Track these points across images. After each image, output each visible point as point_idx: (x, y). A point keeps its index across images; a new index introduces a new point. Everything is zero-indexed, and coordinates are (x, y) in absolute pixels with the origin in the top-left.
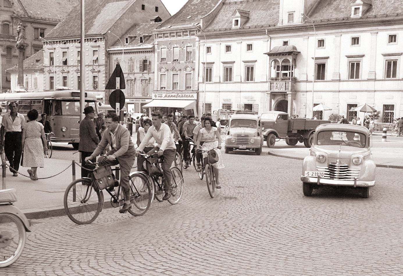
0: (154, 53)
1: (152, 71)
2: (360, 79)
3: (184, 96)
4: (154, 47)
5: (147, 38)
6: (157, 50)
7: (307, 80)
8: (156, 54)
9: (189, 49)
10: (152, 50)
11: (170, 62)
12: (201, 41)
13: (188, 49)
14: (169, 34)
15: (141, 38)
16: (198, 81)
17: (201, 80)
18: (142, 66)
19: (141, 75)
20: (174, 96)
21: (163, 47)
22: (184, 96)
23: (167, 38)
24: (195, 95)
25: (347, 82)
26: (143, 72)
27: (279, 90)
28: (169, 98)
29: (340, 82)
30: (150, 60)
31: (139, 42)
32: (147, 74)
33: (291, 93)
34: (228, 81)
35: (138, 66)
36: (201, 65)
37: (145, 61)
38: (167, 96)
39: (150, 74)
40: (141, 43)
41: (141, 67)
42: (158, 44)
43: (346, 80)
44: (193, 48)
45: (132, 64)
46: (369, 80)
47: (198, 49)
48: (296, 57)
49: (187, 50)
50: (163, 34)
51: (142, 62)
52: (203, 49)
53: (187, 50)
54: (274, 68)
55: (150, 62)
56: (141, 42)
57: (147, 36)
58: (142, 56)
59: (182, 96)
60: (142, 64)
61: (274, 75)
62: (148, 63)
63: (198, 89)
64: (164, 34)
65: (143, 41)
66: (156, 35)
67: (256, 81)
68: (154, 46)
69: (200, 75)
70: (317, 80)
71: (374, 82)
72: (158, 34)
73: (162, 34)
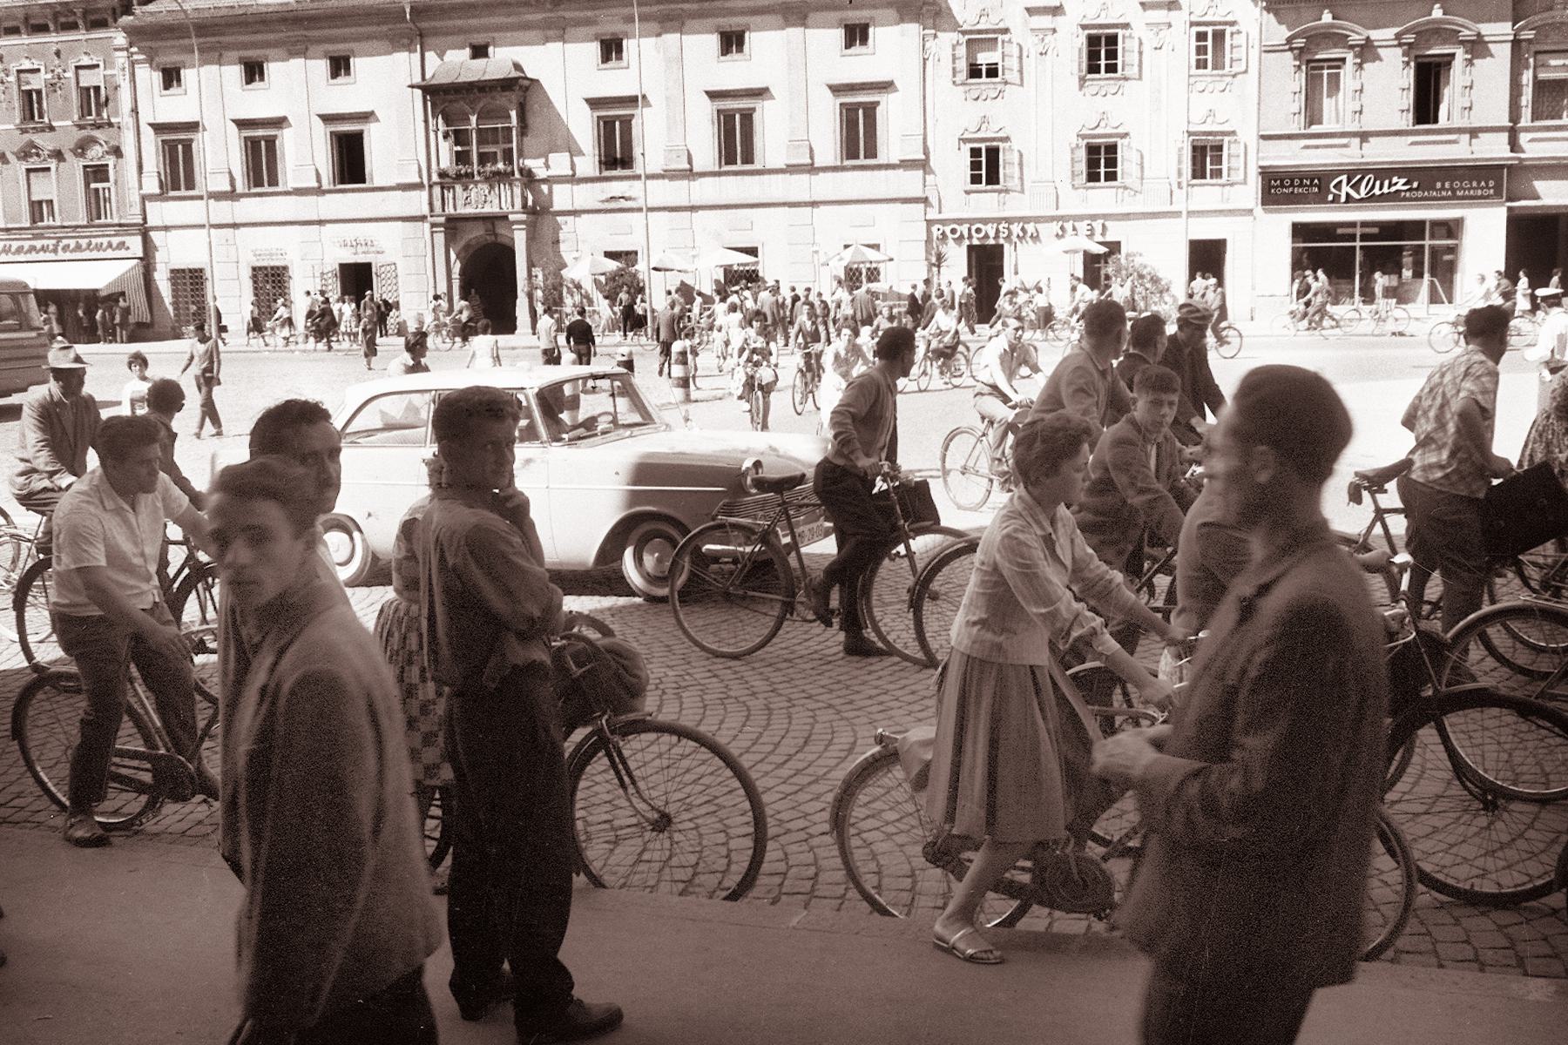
2: (757, 166)
3: (84, 246)
9: (88, 79)
13: (81, 79)
16: (141, 187)
17: (152, 186)
20: (44, 249)
22: (84, 246)
24: (135, 244)
25: (717, 178)
27: (478, 211)
28: (22, 257)
33: (524, 217)
36: (148, 135)
38: (13, 249)
44: (109, 72)
47: (127, 77)
49: (78, 83)
53: (78, 83)
54: (446, 136)
59: (78, 248)
61: (446, 161)
63: (145, 219)
67: (377, 183)
69: (145, 169)
70: (607, 173)
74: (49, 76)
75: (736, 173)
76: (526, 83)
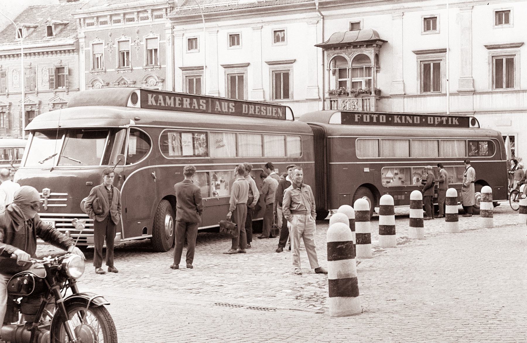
0: (78, 54)
1: (76, 87)
2: (516, 88)
4: (78, 42)
5: (60, 27)
6: (85, 49)
7: (405, 94)
8: (82, 55)
9: (152, 45)
10: (75, 49)
11: (114, 70)
12: (178, 28)
13: (148, 45)
14: (109, 17)
15: (49, 28)
18: (54, 78)
19: (52, 95)
21: (96, 41)
23: (104, 26)
25: (490, 95)
26: (57, 90)
29: (475, 96)
30: (70, 66)
31: (46, 34)
32: (65, 93)
34: (432, 90)
35: (47, 78)
36: (179, 73)
37: (59, 70)
39: (70, 93)
40: (50, 37)
41: (52, 80)
42: (85, 37)
43: (416, 94)
44: (161, 42)
45: (33, 75)
46: (460, 93)
47: (171, 44)
48: (379, 51)
49: (147, 48)
50: (95, 18)
51: (54, 71)
52: (182, 43)
53: (147, 48)
54: (334, 74)
55: (70, 71)
56: (50, 34)
57: (61, 24)
58: (54, 61)
60: (54, 74)
61: (334, 86)
62: (66, 72)
64: (98, 17)
65: (54, 33)
66: (82, 20)
67: (295, 98)
68: (78, 40)
70: (424, 94)
71: (471, 96)
72: (85, 19)
73: (93, 18)
74: (133, 44)
75: (502, 92)
76: (380, 43)
